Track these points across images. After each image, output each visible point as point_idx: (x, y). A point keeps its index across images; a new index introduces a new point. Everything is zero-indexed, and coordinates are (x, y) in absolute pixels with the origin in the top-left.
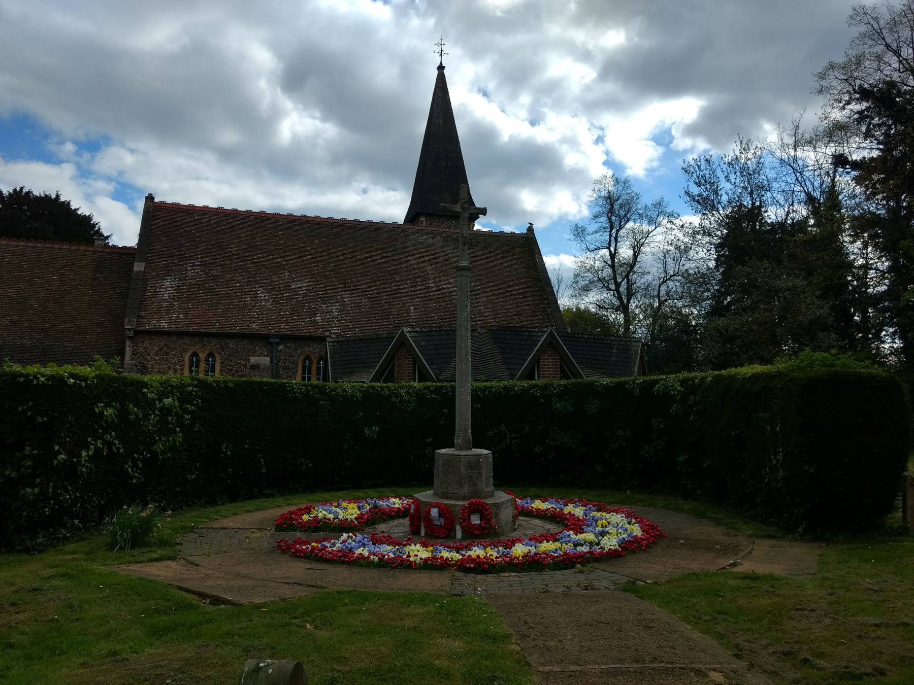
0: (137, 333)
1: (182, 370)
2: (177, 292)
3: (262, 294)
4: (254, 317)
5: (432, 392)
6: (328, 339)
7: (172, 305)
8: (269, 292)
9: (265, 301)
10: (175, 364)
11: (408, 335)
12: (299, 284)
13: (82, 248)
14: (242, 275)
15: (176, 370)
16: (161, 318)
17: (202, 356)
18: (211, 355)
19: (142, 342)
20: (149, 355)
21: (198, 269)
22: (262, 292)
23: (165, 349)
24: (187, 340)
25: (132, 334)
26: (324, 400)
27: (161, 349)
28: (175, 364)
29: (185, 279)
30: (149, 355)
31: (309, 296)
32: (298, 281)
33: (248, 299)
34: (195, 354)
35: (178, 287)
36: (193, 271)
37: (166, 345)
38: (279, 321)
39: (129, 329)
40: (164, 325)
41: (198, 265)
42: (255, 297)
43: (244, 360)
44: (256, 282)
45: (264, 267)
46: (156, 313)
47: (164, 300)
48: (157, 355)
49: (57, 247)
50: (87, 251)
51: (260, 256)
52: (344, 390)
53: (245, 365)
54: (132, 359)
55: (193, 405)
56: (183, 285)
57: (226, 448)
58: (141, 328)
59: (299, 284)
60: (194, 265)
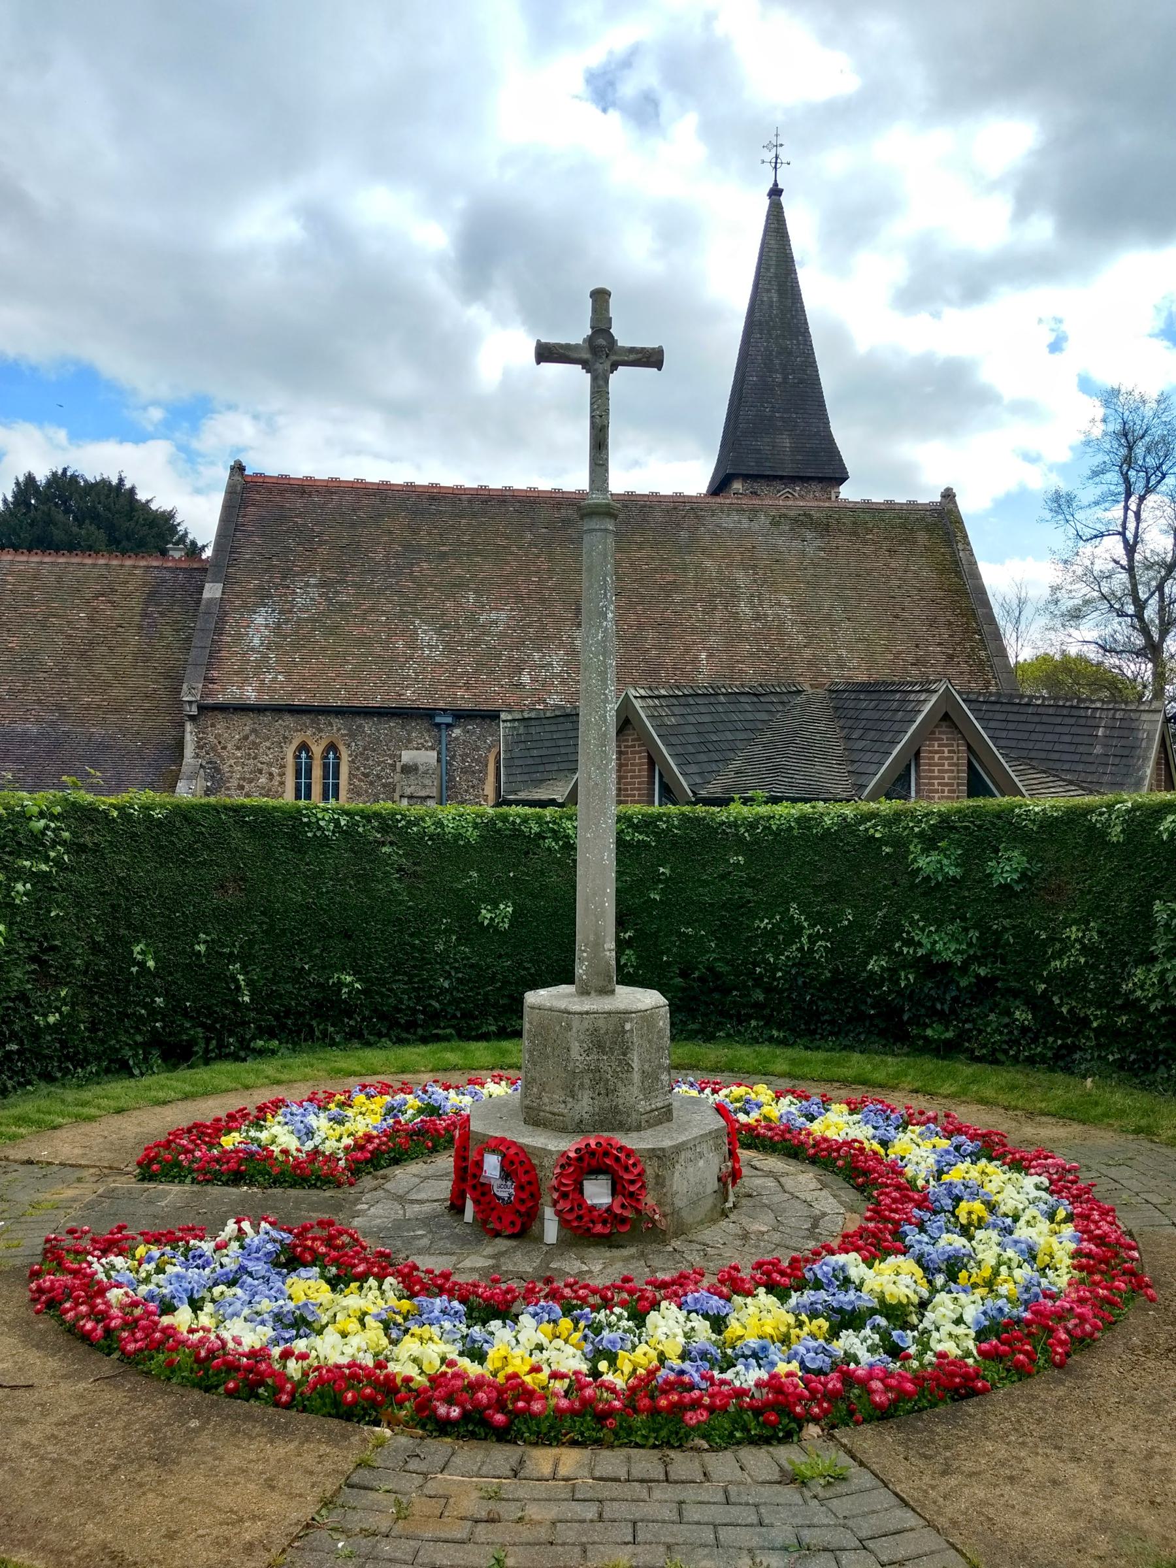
0: (202, 708)
1: (282, 775)
2: (277, 635)
3: (426, 635)
4: (408, 677)
5: (636, 828)
6: (503, 716)
7: (265, 657)
8: (438, 632)
9: (430, 647)
10: (270, 765)
11: (638, 704)
12: (493, 616)
13: (128, 562)
14: (390, 602)
15: (271, 774)
16: (245, 681)
17: (317, 750)
18: (332, 747)
19: (213, 725)
20: (224, 748)
21: (314, 593)
22: (425, 632)
23: (252, 737)
24: (289, 720)
25: (194, 711)
26: (392, 843)
27: (246, 738)
28: (270, 765)
29: (291, 612)
30: (224, 748)
31: (511, 636)
32: (492, 609)
33: (400, 644)
34: (304, 747)
35: (278, 625)
36: (306, 596)
37: (254, 731)
38: (453, 685)
39: (190, 702)
40: (250, 695)
41: (315, 586)
42: (412, 644)
43: (391, 756)
44: (416, 614)
45: (430, 584)
46: (237, 673)
47: (253, 649)
48: (238, 748)
49: (89, 561)
50: (135, 567)
51: (425, 565)
52: (439, 824)
53: (393, 766)
54: (197, 756)
55: (47, 859)
56: (287, 621)
57: (142, 952)
58: (210, 701)
59: (493, 616)
60: (307, 585)
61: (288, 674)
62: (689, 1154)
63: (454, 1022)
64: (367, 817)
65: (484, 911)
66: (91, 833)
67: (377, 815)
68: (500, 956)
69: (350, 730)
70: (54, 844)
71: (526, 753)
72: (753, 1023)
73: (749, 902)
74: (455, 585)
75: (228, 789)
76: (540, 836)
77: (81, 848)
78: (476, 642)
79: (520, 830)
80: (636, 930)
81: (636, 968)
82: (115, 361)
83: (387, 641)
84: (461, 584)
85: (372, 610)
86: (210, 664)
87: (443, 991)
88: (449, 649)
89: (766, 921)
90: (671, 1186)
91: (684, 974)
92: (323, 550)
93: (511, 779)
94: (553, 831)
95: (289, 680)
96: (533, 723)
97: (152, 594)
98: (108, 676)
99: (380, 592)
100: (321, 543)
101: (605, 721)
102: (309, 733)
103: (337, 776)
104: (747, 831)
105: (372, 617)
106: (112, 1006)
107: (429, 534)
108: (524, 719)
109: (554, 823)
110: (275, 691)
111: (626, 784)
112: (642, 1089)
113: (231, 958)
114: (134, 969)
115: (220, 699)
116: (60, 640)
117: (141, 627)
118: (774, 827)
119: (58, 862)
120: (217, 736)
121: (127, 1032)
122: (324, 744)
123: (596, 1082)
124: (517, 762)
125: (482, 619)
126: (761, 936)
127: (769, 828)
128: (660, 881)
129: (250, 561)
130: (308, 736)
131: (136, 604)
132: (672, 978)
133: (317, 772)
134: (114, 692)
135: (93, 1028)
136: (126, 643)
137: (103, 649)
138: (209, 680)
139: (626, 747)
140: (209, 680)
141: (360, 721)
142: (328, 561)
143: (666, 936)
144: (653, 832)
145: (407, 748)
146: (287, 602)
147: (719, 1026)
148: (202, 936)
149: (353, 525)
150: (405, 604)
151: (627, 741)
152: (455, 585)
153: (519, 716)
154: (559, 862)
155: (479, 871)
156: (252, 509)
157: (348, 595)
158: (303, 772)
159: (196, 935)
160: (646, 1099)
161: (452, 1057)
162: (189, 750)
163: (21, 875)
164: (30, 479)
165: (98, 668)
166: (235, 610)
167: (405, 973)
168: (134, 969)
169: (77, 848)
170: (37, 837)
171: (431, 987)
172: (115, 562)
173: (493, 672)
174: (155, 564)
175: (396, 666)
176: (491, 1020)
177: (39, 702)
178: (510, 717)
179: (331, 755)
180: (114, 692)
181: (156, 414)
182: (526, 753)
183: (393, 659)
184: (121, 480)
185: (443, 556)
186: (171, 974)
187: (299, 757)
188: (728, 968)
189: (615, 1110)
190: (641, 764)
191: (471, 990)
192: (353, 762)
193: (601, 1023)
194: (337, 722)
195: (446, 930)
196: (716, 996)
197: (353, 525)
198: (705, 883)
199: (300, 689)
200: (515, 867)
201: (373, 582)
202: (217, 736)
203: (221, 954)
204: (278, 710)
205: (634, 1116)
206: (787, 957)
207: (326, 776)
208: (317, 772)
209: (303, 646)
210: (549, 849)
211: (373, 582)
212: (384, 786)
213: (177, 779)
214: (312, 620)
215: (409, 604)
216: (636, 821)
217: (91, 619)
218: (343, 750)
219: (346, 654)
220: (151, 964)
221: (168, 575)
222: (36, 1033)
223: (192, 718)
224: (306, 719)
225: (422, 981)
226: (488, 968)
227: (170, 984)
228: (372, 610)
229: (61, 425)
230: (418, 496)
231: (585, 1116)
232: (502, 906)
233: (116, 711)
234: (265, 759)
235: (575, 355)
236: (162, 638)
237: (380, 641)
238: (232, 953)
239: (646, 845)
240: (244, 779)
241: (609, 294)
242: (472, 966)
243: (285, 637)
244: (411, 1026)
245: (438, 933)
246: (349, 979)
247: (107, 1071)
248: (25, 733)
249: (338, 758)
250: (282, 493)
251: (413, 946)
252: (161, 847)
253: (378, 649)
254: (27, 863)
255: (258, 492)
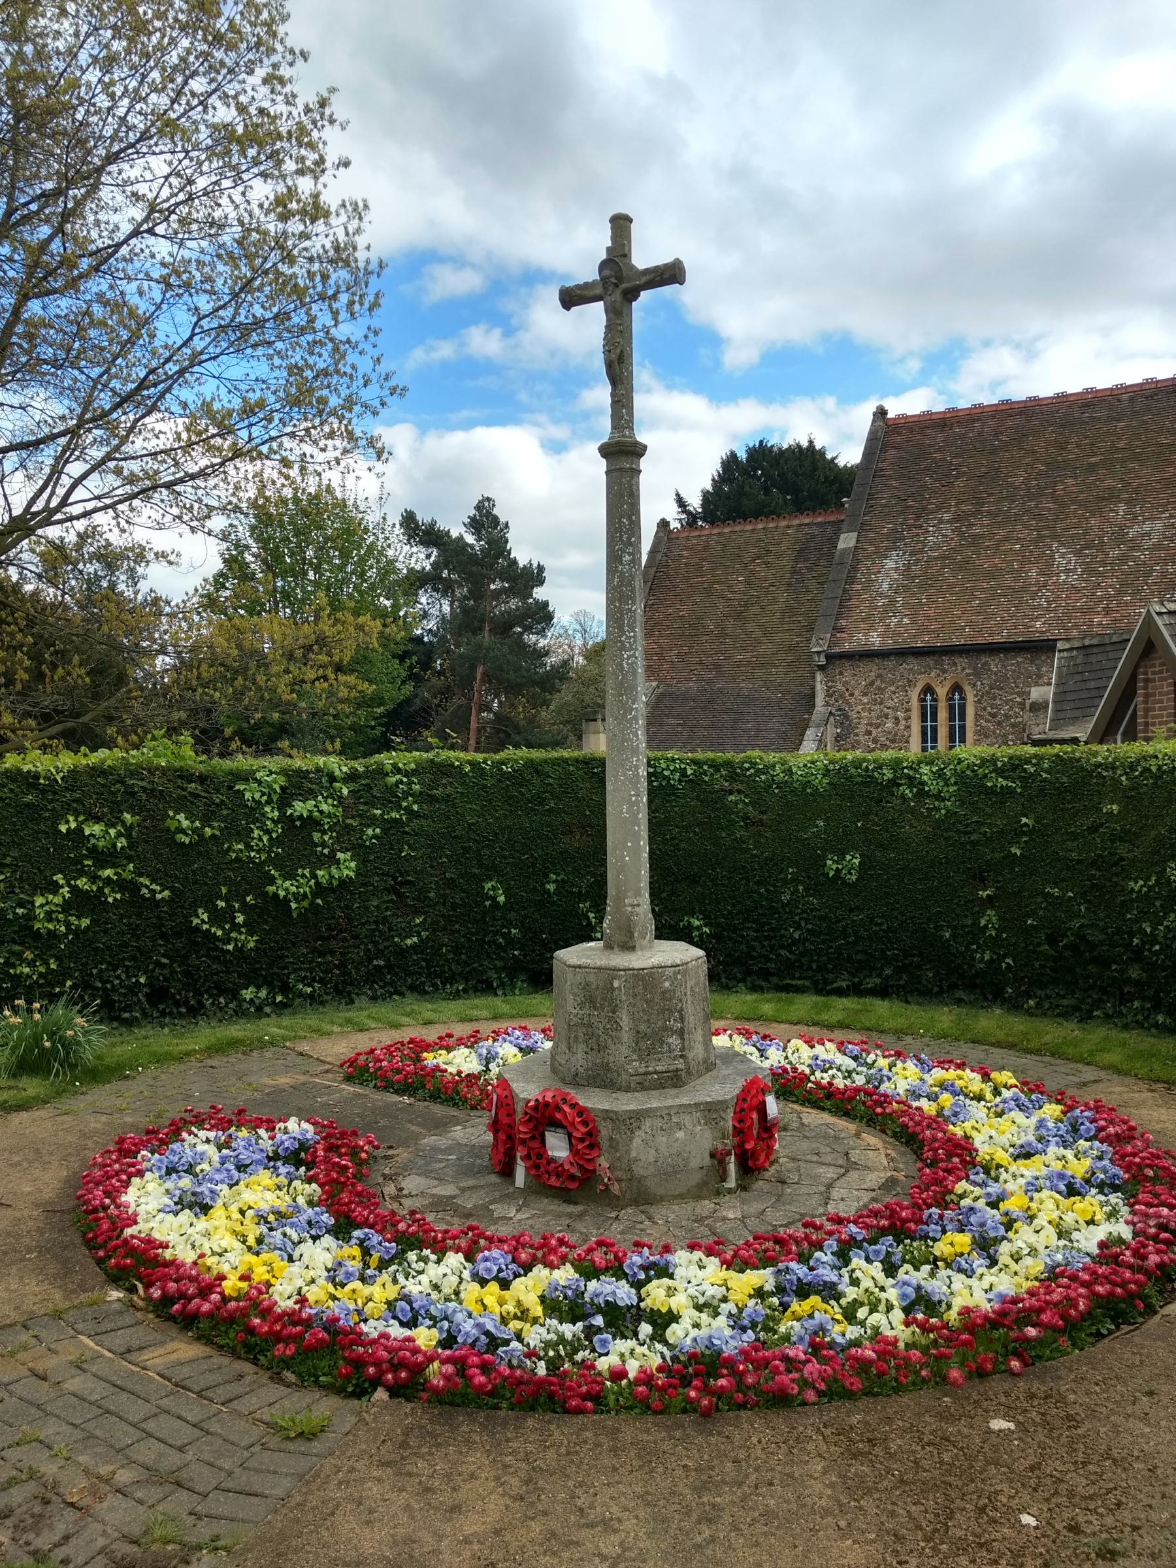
0: (830, 658)
1: (908, 718)
2: (906, 577)
3: (1063, 558)
4: (1040, 607)
5: (1000, 772)
6: (1060, 645)
7: (893, 601)
8: (1078, 553)
9: (1067, 571)
10: (895, 709)
11: (1159, 621)
12: (1147, 527)
13: (783, 523)
14: (1027, 528)
15: (897, 718)
16: (872, 627)
17: (942, 691)
18: (957, 688)
19: (841, 673)
20: (852, 695)
21: (947, 529)
22: (1063, 556)
23: (878, 683)
24: (913, 663)
25: (822, 661)
26: (739, 792)
27: (872, 683)
28: (895, 709)
29: (922, 552)
30: (852, 695)
31: (1167, 548)
32: (1145, 520)
33: (1033, 573)
34: (928, 689)
35: (908, 567)
36: (938, 534)
37: (879, 676)
38: (1091, 611)
39: (819, 653)
40: (875, 640)
41: (948, 522)
42: (1047, 570)
43: (1020, 694)
44: (1055, 537)
45: (1074, 502)
46: (864, 620)
47: (881, 595)
48: (865, 694)
49: (749, 527)
50: (788, 527)
51: (1070, 482)
52: (789, 772)
53: (1022, 705)
54: (827, 704)
55: (399, 808)
56: (917, 562)
57: (494, 888)
58: (837, 650)
59: (1147, 527)
60: (941, 521)
61: (914, 618)
62: (659, 1123)
63: (810, 974)
64: (715, 766)
65: (829, 862)
66: (445, 786)
67: (728, 764)
68: (851, 910)
69: (975, 668)
70: (407, 794)
71: (1082, 686)
72: (1136, 1004)
73: (1122, 859)
74: (1103, 499)
75: (857, 735)
76: (894, 783)
77: (433, 799)
78: (1123, 559)
79: (872, 777)
80: (997, 888)
81: (1000, 931)
82: (870, 322)
83: (1020, 571)
84: (1112, 497)
85: (1006, 539)
86: (840, 613)
87: (795, 942)
88: (1089, 571)
89: (1141, 883)
90: (628, 1152)
91: (1052, 941)
92: (960, 483)
93: (1061, 715)
94: (909, 777)
95: (914, 622)
96: (1095, 650)
97: (801, 551)
98: (758, 633)
99: (1017, 518)
100: (957, 477)
101: (622, 668)
102: (933, 675)
103: (963, 717)
104: (1126, 774)
105: (1006, 547)
106: (473, 934)
107: (1078, 446)
108: (1084, 647)
109: (911, 768)
110: (899, 634)
111: (1154, 717)
112: (637, 1049)
113: (581, 897)
114: (488, 903)
115: (847, 647)
116: (721, 604)
117: (789, 584)
118: (1154, 769)
119: (409, 811)
120: (845, 684)
121: (489, 956)
122: (948, 685)
123: (590, 1036)
124: (1069, 697)
125: (1132, 533)
126: (1137, 900)
127: (1149, 770)
128: (1024, 833)
129: (885, 506)
130: (931, 678)
131: (787, 563)
132: (1039, 945)
133: (943, 715)
134: (763, 649)
135: (457, 950)
136: (775, 601)
137: (756, 609)
138: (837, 629)
139: (1154, 673)
140: (837, 629)
141: (984, 659)
142: (963, 493)
143: (1030, 896)
144: (1020, 777)
145: (1037, 684)
146: (918, 542)
147: (1099, 1003)
148: (553, 877)
149: (994, 451)
150: (1043, 528)
151: (1154, 666)
152: (1103, 499)
153: (1077, 644)
154: (912, 811)
155: (826, 820)
156: (892, 452)
157: (982, 526)
158: (928, 714)
159: (546, 876)
160: (641, 1059)
161: (767, 1008)
162: (820, 700)
163: (373, 821)
164: (733, 455)
165: (750, 627)
166: (867, 558)
167: (754, 921)
168: (488, 903)
169: (425, 798)
170: (391, 790)
171: (782, 936)
172: (771, 525)
173: (1139, 592)
174: (806, 521)
175: (1026, 596)
176: (846, 975)
177: (701, 662)
178: (1067, 646)
179: (957, 696)
180: (763, 649)
181: (915, 365)
182: (1082, 686)
183: (1024, 589)
184: (811, 442)
185: (1092, 468)
186: (524, 908)
187: (924, 700)
188: (1101, 937)
189: (606, 1067)
190: (1168, 693)
191: (823, 942)
192: (979, 702)
193: (591, 978)
194: (962, 662)
195: (793, 880)
196: (1093, 969)
197: (994, 451)
198: (1075, 836)
199: (925, 630)
200: (865, 816)
201: (1010, 509)
202: (845, 684)
203: (572, 893)
204: (902, 654)
205: (624, 1076)
206: (1167, 927)
207: (952, 718)
208: (943, 715)
209: (931, 586)
210: (903, 797)
211: (1010, 509)
212: (1013, 725)
213: (807, 727)
214: (942, 558)
215: (1047, 528)
216: (999, 764)
217: (748, 582)
218: (968, 689)
219: (974, 589)
220: (502, 899)
221: (816, 530)
222: (402, 952)
223: (822, 668)
224: (930, 661)
225: (772, 930)
226: (838, 921)
227: (525, 917)
228: (1006, 539)
229: (831, 394)
230: (1070, 406)
231: (581, 1070)
232: (848, 857)
233: (763, 665)
234: (890, 703)
235: (591, 293)
236: (808, 592)
237: (1012, 571)
238: (580, 893)
239: (1011, 791)
240: (871, 725)
241: (631, 221)
242: (821, 918)
243: (913, 578)
244: (766, 974)
245: (785, 882)
246: (697, 923)
247: (476, 990)
248: (687, 692)
249: (963, 699)
250: (922, 430)
251: (761, 894)
252: (511, 797)
253: (1009, 581)
254: (379, 812)
255: (899, 434)
